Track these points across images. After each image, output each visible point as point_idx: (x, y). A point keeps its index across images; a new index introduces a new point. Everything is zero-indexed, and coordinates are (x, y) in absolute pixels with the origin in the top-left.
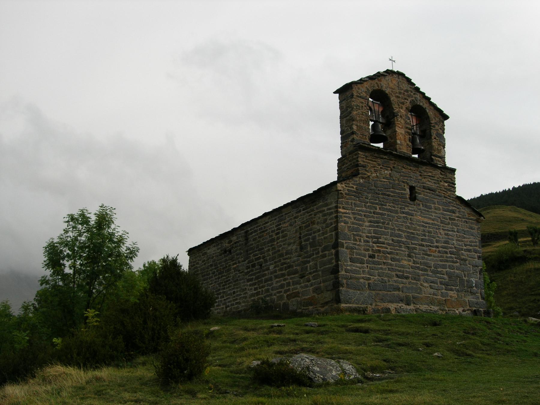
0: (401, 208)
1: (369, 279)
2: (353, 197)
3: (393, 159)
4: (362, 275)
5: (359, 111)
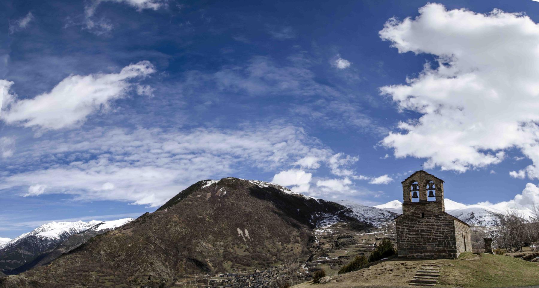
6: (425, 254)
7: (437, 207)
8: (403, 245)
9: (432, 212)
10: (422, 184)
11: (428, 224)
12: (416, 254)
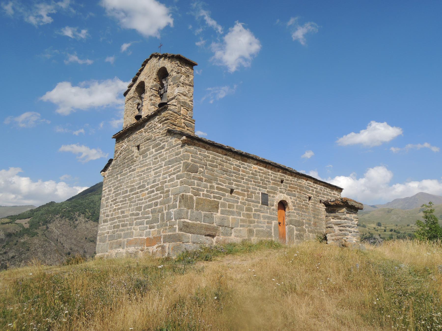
7: (160, 123)
11: (143, 169)
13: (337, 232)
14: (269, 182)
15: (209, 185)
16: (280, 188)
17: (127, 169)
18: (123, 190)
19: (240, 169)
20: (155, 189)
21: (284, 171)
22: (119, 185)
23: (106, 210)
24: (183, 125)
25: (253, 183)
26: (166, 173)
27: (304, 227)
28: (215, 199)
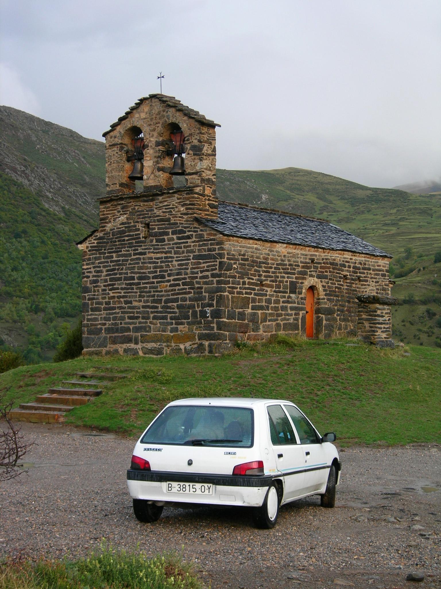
0: (135, 250)
1: (105, 324)
2: (94, 252)
3: (130, 201)
4: (100, 322)
5: (111, 161)
6: (144, 345)
7: (183, 206)
8: (96, 319)
9: (169, 220)
10: (152, 136)
11: (159, 255)
12: (125, 346)
13: (368, 328)
14: (298, 266)
15: (241, 281)
16: (310, 271)
17: (130, 249)
18: (126, 276)
19: (269, 257)
20: (180, 282)
21: (316, 249)
22: (117, 267)
23: (94, 295)
24: (207, 207)
25: (281, 270)
26: (198, 268)
27: (335, 315)
28: (247, 296)
